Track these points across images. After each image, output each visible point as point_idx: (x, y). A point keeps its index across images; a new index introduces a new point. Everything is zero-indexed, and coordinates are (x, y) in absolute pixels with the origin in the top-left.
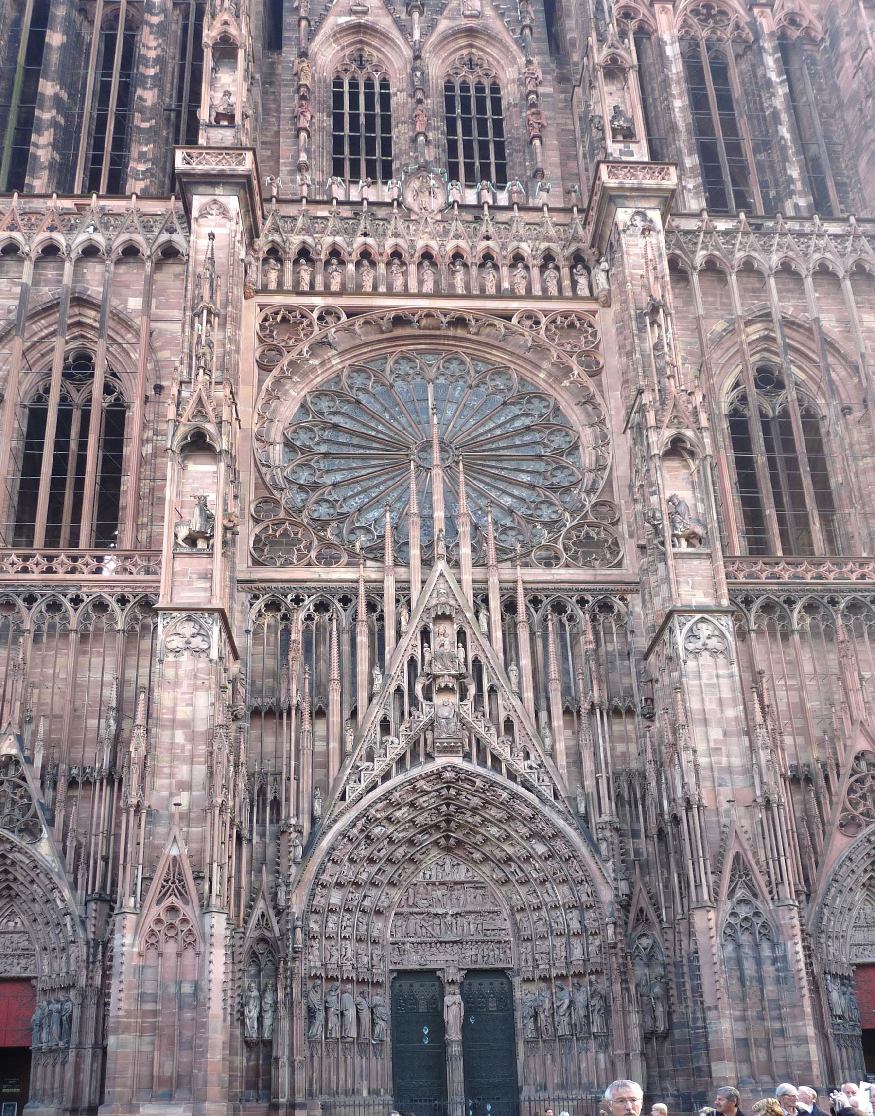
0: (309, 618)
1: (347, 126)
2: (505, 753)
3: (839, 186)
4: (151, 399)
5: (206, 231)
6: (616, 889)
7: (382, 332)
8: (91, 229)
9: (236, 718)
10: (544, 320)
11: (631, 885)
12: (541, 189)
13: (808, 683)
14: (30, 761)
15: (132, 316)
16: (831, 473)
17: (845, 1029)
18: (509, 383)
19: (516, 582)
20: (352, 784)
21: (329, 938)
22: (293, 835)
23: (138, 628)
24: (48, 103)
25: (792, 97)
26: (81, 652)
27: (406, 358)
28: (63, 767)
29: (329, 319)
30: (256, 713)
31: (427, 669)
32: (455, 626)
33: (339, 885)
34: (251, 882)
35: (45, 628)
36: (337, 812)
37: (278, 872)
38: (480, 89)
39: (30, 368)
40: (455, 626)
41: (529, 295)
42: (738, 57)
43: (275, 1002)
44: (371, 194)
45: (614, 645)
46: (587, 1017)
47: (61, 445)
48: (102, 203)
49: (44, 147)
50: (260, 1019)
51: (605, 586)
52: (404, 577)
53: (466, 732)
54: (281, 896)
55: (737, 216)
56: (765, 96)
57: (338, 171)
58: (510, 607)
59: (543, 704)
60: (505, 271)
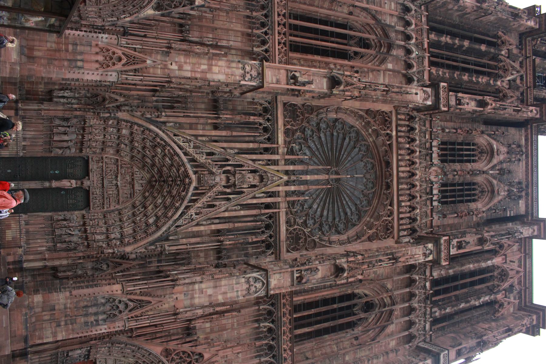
0: (261, 124)
1: (459, 147)
2: (199, 205)
3: (443, 327)
4: (353, 69)
5: (419, 92)
6: (132, 253)
7: (383, 157)
8: (417, 53)
9: (213, 92)
10: (390, 219)
11: (134, 260)
12: (439, 217)
13: (235, 332)
14: (192, 9)
15: (385, 65)
16: (330, 335)
17: (61, 358)
18: (364, 206)
19: (279, 209)
20: (182, 139)
21: (105, 129)
22: (156, 114)
23: (254, 56)
24: (461, 43)
25: (475, 307)
26: (243, 34)
27: (373, 167)
28: (189, 22)
29: (387, 137)
30: (216, 101)
31: (238, 172)
32: (258, 184)
33: (132, 133)
34: (133, 96)
35: (254, 20)
36: (169, 133)
37: (138, 107)
38: (474, 195)
39: (363, 26)
40: (258, 184)
41: (399, 213)
42: (488, 287)
43: (72, 104)
44: (435, 155)
45: (250, 251)
46: (65, 242)
47: (332, 34)
48: (427, 58)
49: (446, 39)
50: (63, 97)
51: (278, 246)
52: (280, 163)
53: (208, 188)
54: (127, 108)
55: (431, 290)
56: (475, 297)
57: (443, 143)
58: (268, 206)
59: (222, 221)
60: (408, 204)
